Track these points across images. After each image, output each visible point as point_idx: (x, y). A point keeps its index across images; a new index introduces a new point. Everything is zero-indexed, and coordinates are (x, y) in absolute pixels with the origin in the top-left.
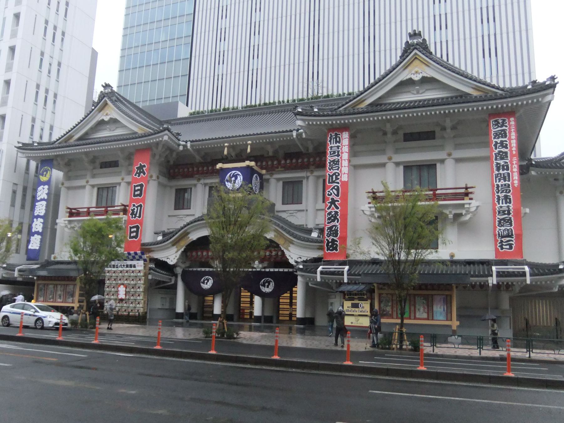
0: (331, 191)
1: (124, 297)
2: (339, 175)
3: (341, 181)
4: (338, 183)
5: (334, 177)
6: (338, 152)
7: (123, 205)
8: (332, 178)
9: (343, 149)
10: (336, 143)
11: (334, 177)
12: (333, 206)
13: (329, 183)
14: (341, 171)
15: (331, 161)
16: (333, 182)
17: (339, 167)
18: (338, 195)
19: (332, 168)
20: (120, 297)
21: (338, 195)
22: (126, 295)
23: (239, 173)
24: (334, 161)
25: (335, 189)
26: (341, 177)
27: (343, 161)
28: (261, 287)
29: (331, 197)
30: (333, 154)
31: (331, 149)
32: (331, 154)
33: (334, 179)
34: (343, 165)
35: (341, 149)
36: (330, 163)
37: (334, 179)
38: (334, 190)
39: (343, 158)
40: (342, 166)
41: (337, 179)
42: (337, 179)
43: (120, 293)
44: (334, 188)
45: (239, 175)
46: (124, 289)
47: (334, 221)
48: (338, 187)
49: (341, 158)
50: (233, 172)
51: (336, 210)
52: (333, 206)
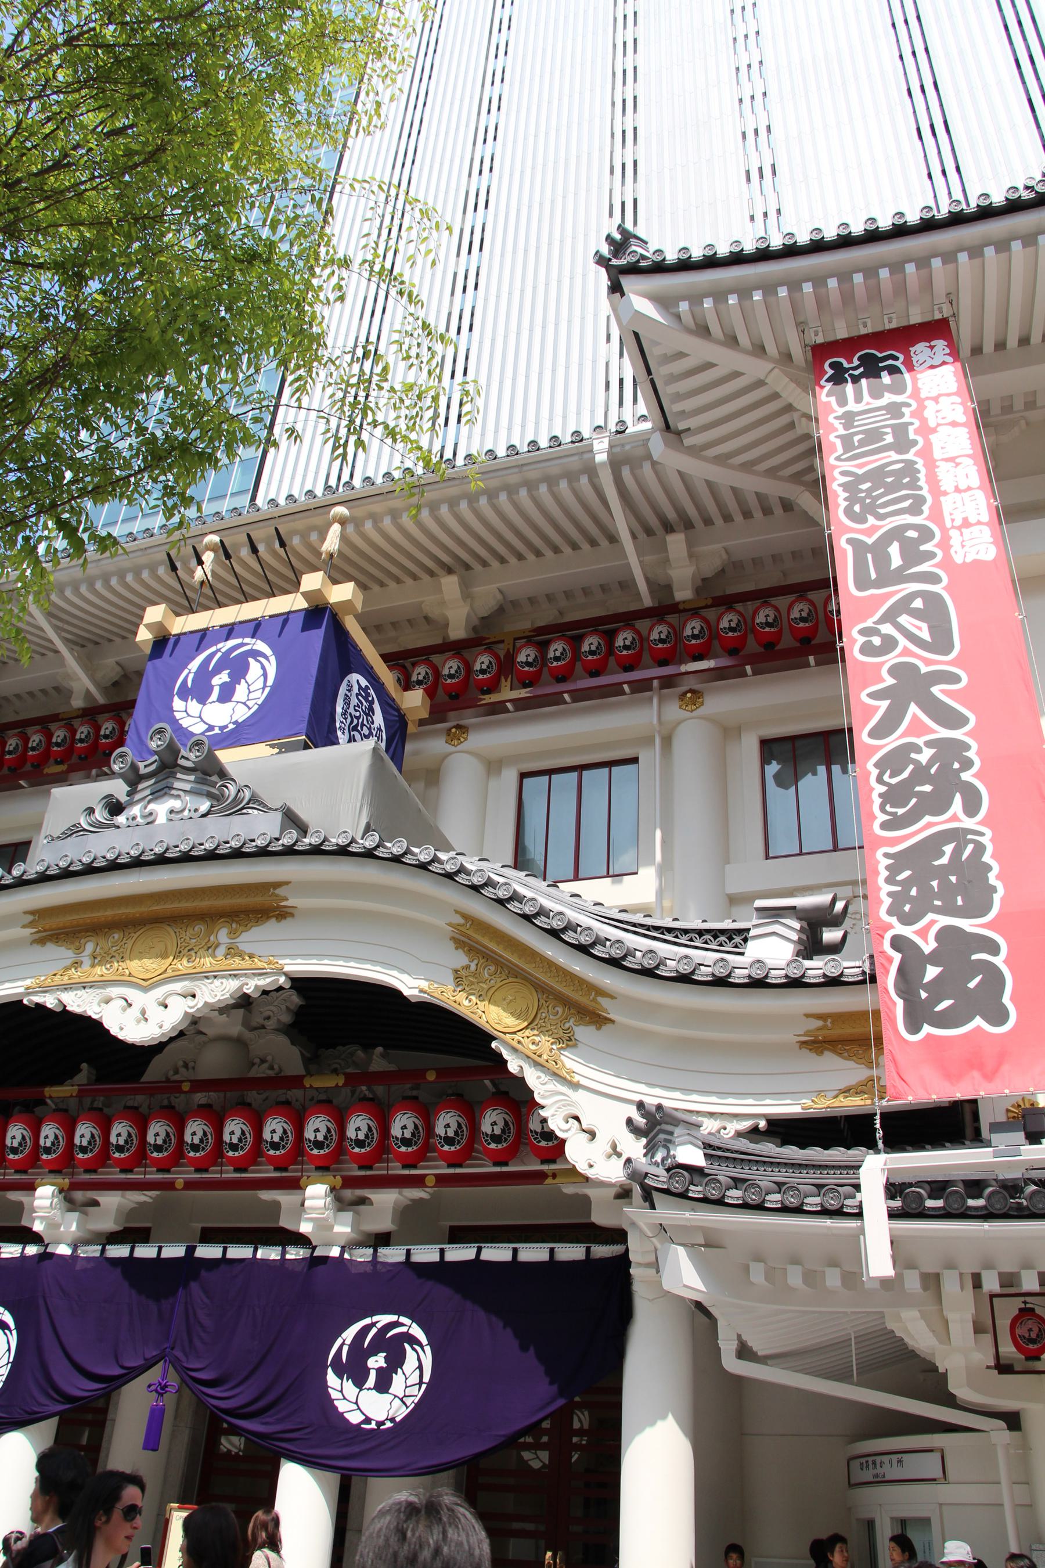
0: (887, 629)
3: (947, 563)
4: (934, 579)
8: (883, 560)
12: (913, 709)
13: (862, 583)
18: (941, 643)
21: (941, 643)
25: (915, 614)
26: (945, 544)
28: (332, 1379)
29: (892, 659)
33: (896, 561)
37: (896, 561)
38: (904, 620)
44: (903, 606)
48: (934, 601)
51: (944, 733)
52: (913, 709)
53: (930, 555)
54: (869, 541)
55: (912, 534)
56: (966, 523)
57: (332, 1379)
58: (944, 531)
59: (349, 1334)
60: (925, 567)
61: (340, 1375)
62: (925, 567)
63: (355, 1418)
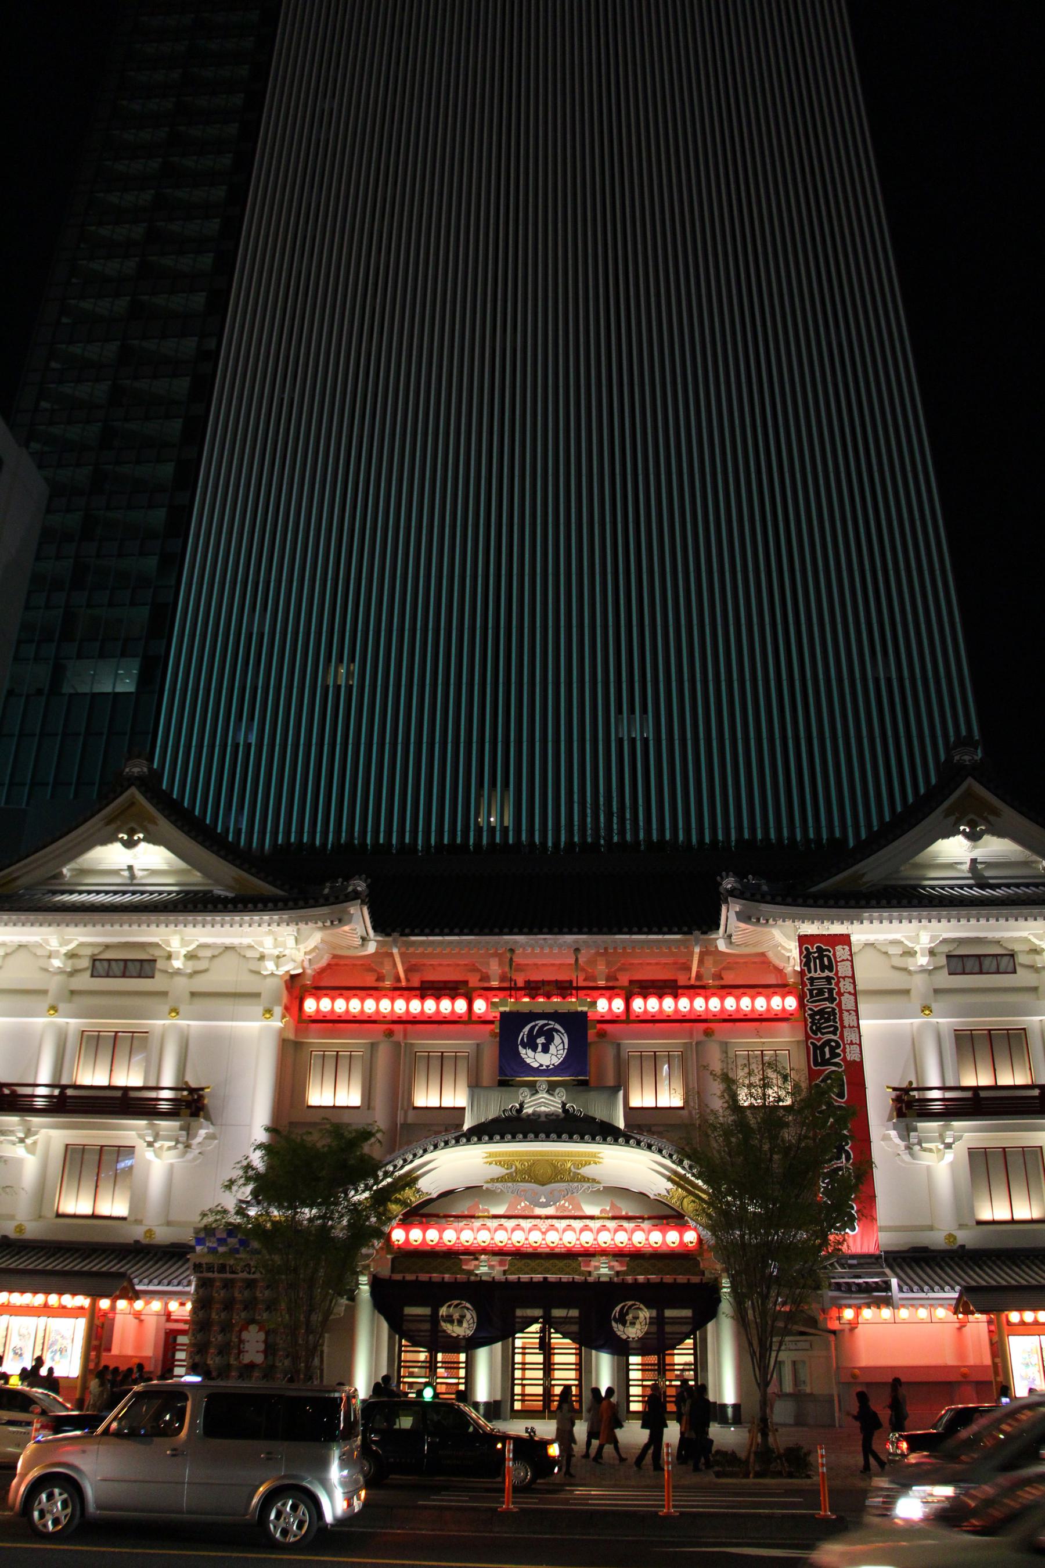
1: (259, 1359)
2: (838, 1046)
3: (844, 1059)
5: (827, 1049)
6: (831, 991)
7: (192, 1091)
8: (823, 1054)
9: (841, 985)
10: (823, 971)
11: (827, 1049)
14: (842, 1037)
15: (815, 1013)
16: (826, 1062)
17: (836, 1028)
19: (819, 1029)
20: (246, 1359)
22: (265, 1352)
23: (558, 1027)
24: (822, 1012)
26: (844, 1051)
27: (845, 1014)
30: (817, 995)
31: (812, 985)
32: (812, 996)
33: (828, 1056)
34: (846, 1024)
35: (837, 984)
36: (812, 1016)
37: (828, 1056)
39: (843, 1007)
40: (843, 1027)
41: (834, 1055)
42: (834, 1055)
43: (247, 1346)
45: (557, 1031)
46: (262, 1336)
47: (839, 1158)
49: (839, 1005)
50: (541, 1022)
53: (839, 1055)
54: (819, 1044)
55: (833, 1044)
56: (852, 1043)
57: (614, 1324)
58: (844, 1045)
59: (618, 1308)
60: (836, 1060)
61: (616, 1322)
62: (836, 1060)
63: (624, 1337)
